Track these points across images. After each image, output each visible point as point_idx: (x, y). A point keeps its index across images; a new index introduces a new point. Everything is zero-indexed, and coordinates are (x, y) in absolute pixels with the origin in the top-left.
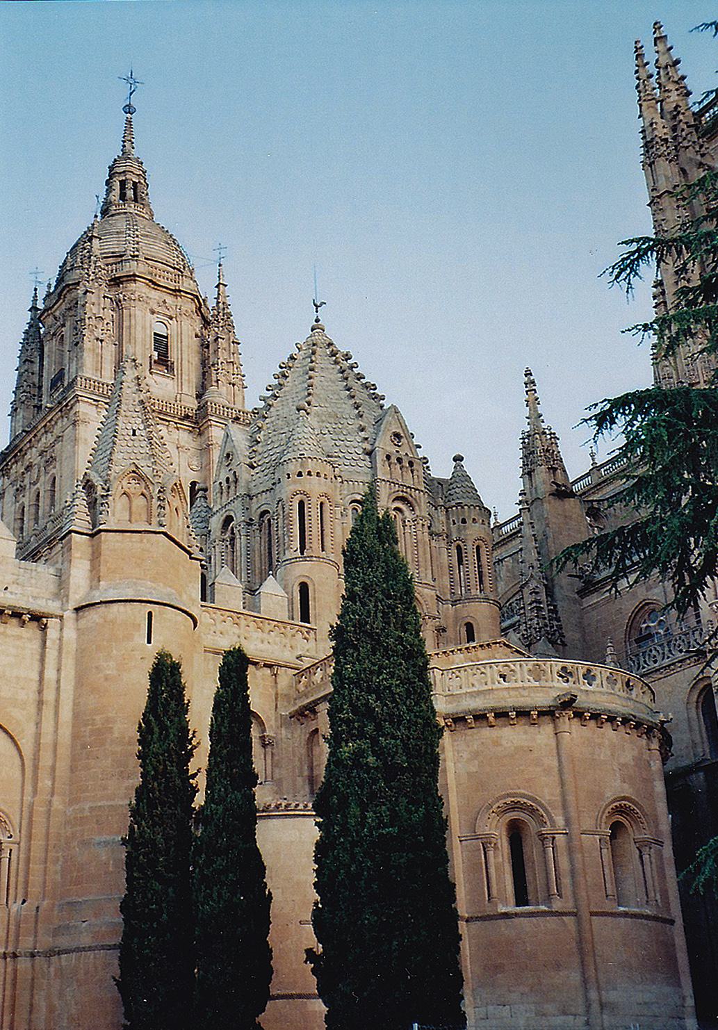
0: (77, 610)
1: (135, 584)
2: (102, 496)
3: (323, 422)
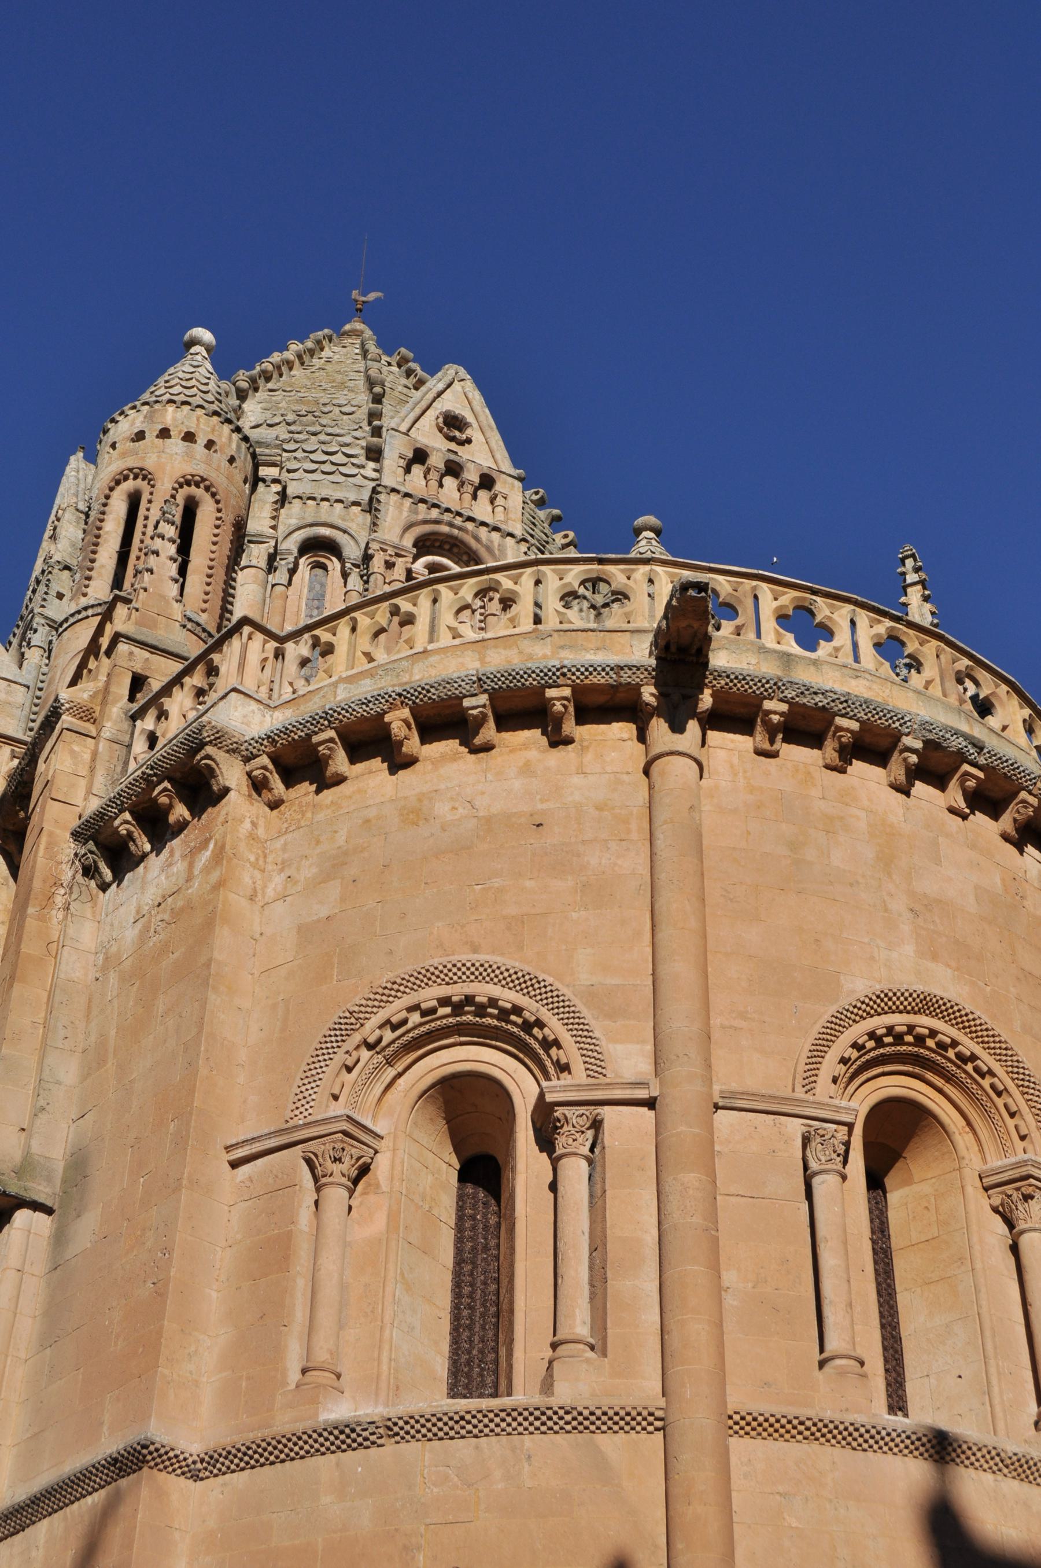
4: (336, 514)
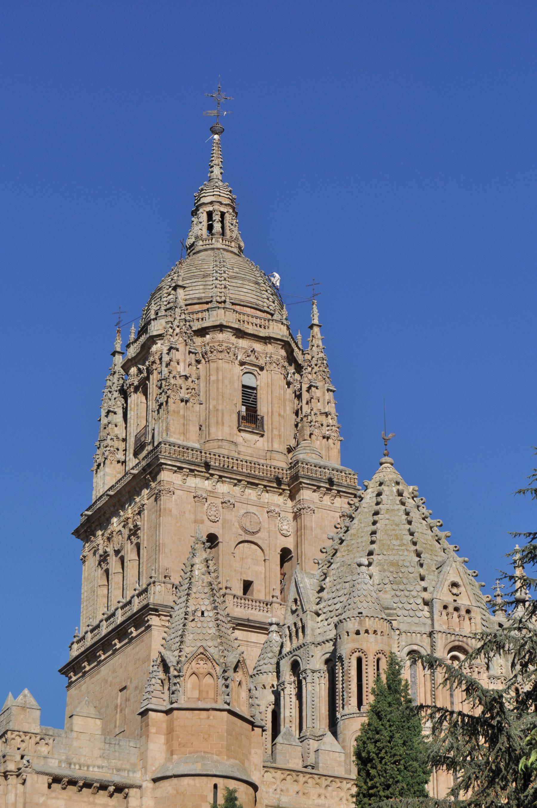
0: (155, 780)
1: (203, 758)
2: (175, 677)
3: (384, 571)
4: (417, 639)
